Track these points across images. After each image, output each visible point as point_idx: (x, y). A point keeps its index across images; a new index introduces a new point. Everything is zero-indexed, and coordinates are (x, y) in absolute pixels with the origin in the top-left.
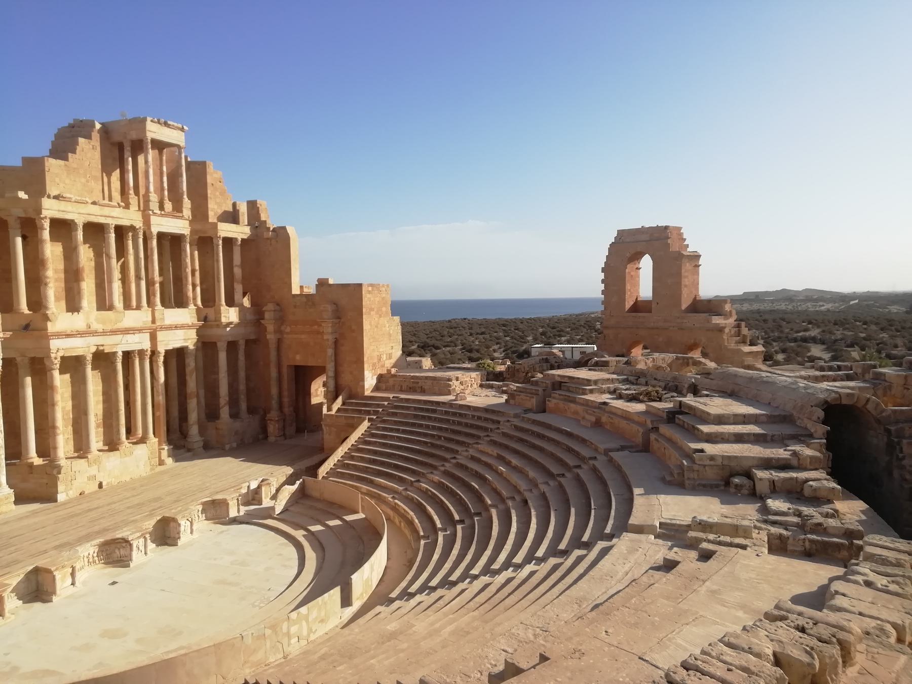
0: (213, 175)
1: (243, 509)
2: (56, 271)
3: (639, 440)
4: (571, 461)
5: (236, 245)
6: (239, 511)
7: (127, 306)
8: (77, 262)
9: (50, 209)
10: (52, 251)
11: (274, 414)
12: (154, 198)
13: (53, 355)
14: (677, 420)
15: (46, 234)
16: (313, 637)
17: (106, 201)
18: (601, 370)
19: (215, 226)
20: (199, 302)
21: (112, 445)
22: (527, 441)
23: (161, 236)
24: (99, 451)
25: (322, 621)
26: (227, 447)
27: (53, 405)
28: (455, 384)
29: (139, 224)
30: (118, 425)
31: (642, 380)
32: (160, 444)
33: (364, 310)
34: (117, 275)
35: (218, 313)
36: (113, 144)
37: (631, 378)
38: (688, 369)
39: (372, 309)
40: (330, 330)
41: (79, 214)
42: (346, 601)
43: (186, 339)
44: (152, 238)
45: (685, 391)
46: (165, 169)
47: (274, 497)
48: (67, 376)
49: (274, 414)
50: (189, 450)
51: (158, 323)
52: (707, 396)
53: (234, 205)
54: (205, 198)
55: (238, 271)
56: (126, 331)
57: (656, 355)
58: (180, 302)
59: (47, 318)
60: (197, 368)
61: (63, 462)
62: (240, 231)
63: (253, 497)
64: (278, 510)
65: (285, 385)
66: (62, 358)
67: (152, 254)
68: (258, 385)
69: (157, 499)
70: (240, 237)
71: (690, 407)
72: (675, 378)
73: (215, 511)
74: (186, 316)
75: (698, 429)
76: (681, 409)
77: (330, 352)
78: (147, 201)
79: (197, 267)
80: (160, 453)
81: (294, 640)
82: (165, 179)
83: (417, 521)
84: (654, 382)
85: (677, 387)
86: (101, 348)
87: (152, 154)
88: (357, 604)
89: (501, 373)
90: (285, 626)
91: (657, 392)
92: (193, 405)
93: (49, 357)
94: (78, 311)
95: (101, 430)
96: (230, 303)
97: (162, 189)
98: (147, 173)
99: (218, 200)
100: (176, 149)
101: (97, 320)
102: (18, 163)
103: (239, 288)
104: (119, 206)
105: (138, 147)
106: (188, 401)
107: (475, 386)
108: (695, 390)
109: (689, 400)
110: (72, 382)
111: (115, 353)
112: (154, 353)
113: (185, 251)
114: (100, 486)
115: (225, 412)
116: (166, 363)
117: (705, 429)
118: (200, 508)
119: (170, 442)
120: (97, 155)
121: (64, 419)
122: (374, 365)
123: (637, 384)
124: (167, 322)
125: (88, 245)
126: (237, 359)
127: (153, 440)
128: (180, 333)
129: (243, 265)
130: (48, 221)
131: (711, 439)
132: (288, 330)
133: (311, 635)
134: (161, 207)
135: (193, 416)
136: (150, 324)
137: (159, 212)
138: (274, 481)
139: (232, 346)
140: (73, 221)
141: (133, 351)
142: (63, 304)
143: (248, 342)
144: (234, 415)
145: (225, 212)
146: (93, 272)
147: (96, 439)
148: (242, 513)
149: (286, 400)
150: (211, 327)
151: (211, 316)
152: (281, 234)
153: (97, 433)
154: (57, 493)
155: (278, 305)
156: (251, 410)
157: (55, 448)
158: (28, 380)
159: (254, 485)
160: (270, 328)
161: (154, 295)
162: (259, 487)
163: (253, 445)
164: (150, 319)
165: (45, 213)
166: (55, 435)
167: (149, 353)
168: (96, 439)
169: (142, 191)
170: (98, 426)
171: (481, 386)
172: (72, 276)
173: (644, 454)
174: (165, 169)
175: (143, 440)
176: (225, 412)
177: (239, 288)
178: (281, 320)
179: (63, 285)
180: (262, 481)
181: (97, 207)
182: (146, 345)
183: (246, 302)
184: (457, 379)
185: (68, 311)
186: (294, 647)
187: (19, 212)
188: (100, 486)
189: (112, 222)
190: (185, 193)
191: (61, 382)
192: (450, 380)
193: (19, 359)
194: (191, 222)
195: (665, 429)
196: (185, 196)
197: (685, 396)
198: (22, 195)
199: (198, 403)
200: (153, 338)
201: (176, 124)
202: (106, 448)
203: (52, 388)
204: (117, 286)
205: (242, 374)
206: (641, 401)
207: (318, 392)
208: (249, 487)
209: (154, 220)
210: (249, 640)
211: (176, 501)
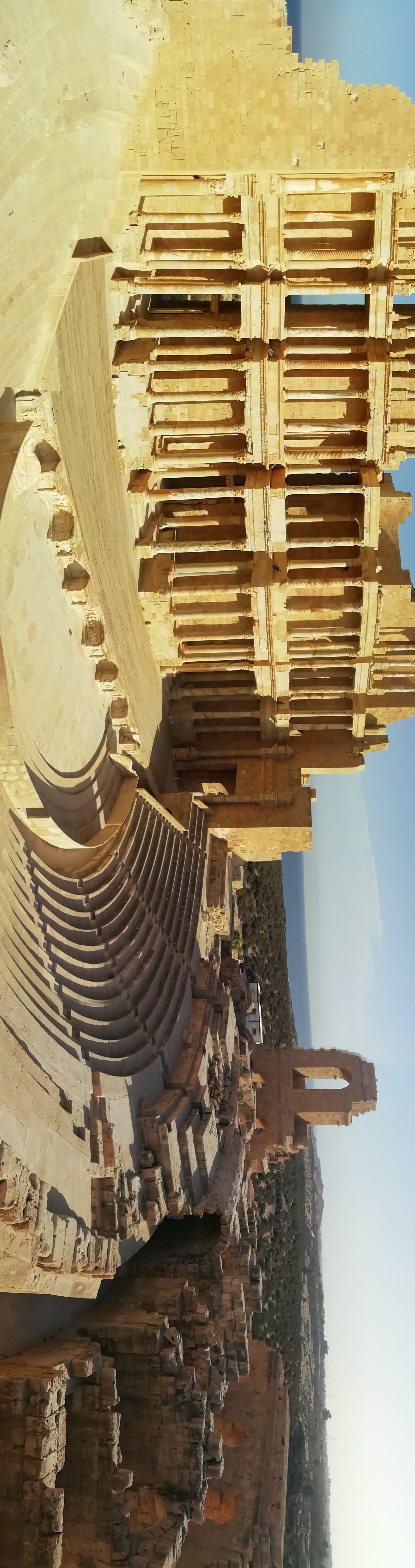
3: (175, 1080)
4: (150, 1021)
14: (194, 1110)
18: (236, 1048)
22: (166, 978)
28: (217, 911)
31: (228, 1083)
37: (230, 1073)
38: (244, 1118)
39: (287, 835)
45: (222, 1116)
52: (219, 1133)
57: (254, 1094)
71: (207, 1121)
72: (233, 1109)
75: (188, 1127)
76: (204, 1115)
84: (227, 1092)
85: (225, 1110)
89: (230, 954)
91: (219, 1095)
107: (217, 930)
108: (223, 1124)
109: (213, 1120)
117: (189, 1132)
123: (225, 1078)
131: (181, 1137)
171: (217, 936)
173: (162, 1084)
184: (222, 913)
192: (221, 906)
195: (185, 1101)
197: (217, 1116)
206: (209, 1082)
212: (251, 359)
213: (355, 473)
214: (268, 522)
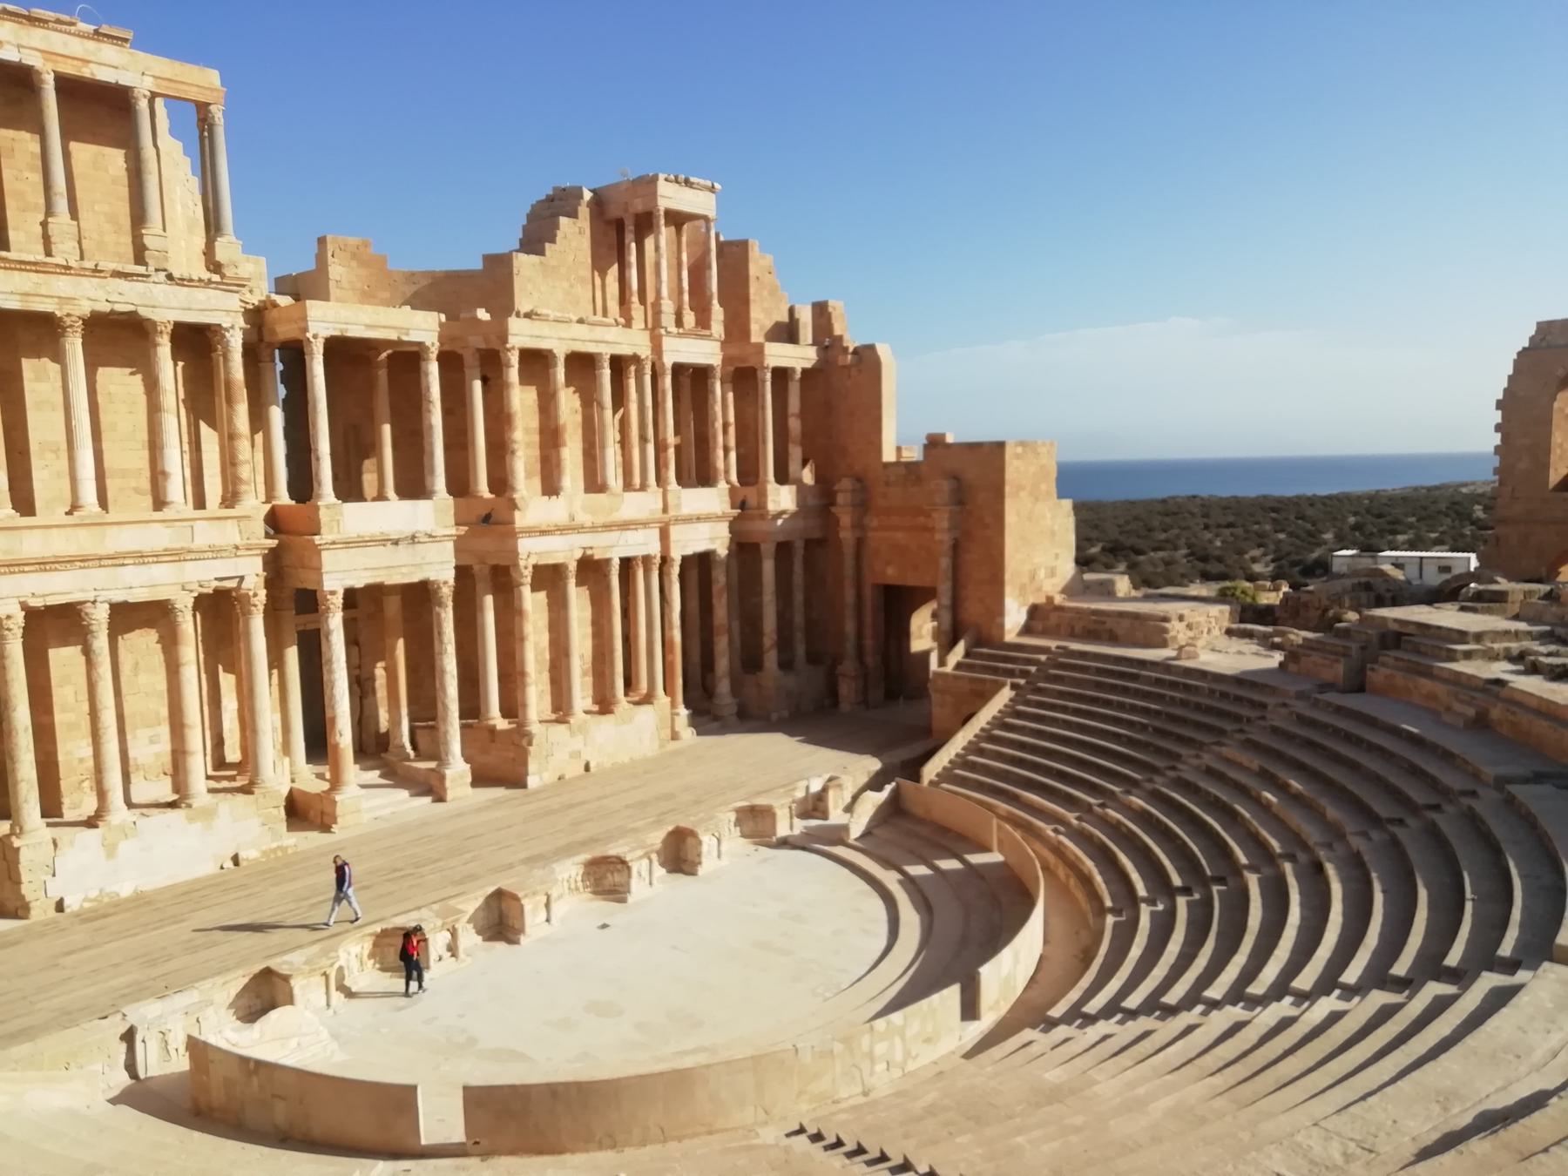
0: (759, 263)
1: (800, 826)
2: (527, 431)
6: (791, 828)
7: (628, 486)
8: (556, 417)
9: (521, 334)
10: (522, 399)
11: (848, 666)
12: (668, 306)
13: (522, 563)
15: (513, 374)
16: (911, 1066)
17: (599, 318)
19: (760, 349)
20: (734, 477)
21: (604, 705)
23: (678, 369)
24: (586, 712)
25: (928, 1040)
26: (774, 716)
27: (522, 639)
28: (1177, 630)
29: (645, 352)
32: (673, 705)
33: (1007, 489)
34: (612, 435)
35: (763, 495)
36: (608, 222)
39: (1022, 488)
40: (945, 524)
41: (560, 341)
42: (970, 1010)
43: (714, 539)
44: (664, 374)
46: (685, 257)
47: (849, 809)
48: (542, 595)
49: (848, 666)
50: (716, 718)
51: (672, 513)
53: (791, 311)
54: (746, 301)
55: (794, 425)
56: (625, 526)
58: (704, 477)
59: (513, 505)
60: (728, 586)
61: (534, 727)
62: (799, 356)
63: (814, 806)
64: (856, 831)
65: (868, 619)
66: (535, 567)
67: (664, 401)
68: (827, 618)
69: (669, 797)
73: (756, 822)
74: (714, 500)
77: (945, 562)
78: (657, 312)
79: (732, 419)
81: (880, 1067)
83: (1098, 879)
86: (589, 552)
87: (665, 233)
88: (989, 1017)
89: (1269, 609)
90: (865, 1041)
92: (722, 644)
93: (516, 565)
94: (557, 494)
95: (589, 679)
96: (782, 477)
97: (681, 292)
98: (657, 265)
100: (702, 223)
102: (478, 265)
103: (796, 453)
104: (617, 324)
105: (645, 224)
106: (716, 639)
107: (1216, 632)
110: (549, 605)
111: (608, 561)
112: (665, 560)
113: (714, 392)
114: (587, 768)
115: (771, 659)
116: (682, 576)
118: (733, 816)
119: (687, 705)
120: (585, 243)
121: (537, 661)
122: (1023, 588)
124: (686, 511)
125: (572, 389)
126: (790, 572)
127: (662, 699)
128: (704, 529)
129: (803, 415)
132: (875, 523)
133: (910, 1062)
134: (679, 322)
135: (722, 664)
136: (659, 515)
137: (673, 329)
138: (847, 780)
140: (550, 351)
141: (634, 558)
142: (537, 483)
143: (809, 544)
144: (786, 665)
145: (778, 325)
146: (580, 431)
147: (582, 694)
148: (797, 832)
149: (869, 643)
151: (752, 501)
152: (867, 358)
153: (582, 684)
154: (526, 774)
155: (859, 480)
156: (813, 658)
157: (524, 706)
158: (489, 600)
159: (816, 786)
160: (845, 519)
161: (666, 466)
162: (825, 790)
163: (816, 718)
164: (660, 506)
166: (524, 686)
167: (658, 561)
168: (582, 694)
169: (651, 297)
170: (584, 674)
172: (550, 437)
174: (685, 257)
175: (648, 699)
176: (771, 659)
177: (796, 453)
178: (863, 505)
179: (537, 452)
180: (830, 780)
181: (584, 326)
182: (655, 549)
183: (808, 476)
184: (1181, 618)
185: (544, 493)
186: (882, 1081)
187: (476, 341)
188: (587, 768)
189: (606, 351)
191: (533, 604)
192: (1166, 619)
193: (476, 568)
196: (715, 301)
198: (483, 315)
199: (731, 642)
200: (664, 536)
201: (702, 181)
202: (596, 708)
203: (520, 612)
204: (612, 454)
205: (799, 598)
207: (922, 631)
208: (808, 788)
209: (668, 343)
210: (806, 1058)
211: (697, 802)
213: (276, 352)
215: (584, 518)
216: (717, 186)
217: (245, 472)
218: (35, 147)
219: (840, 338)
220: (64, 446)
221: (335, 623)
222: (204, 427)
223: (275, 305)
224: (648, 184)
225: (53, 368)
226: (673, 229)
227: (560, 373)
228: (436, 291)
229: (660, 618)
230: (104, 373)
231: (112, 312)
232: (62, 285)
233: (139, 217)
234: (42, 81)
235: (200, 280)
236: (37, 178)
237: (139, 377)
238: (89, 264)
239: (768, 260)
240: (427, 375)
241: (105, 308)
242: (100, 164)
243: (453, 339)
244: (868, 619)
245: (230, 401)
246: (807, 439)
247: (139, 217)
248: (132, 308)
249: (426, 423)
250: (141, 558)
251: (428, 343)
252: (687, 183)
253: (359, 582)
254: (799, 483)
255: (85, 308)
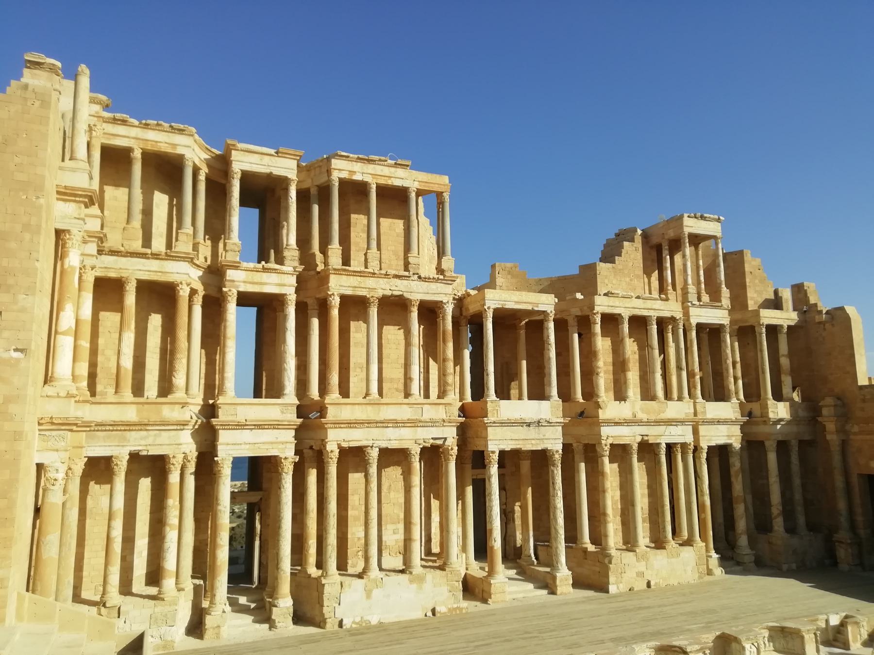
0: (751, 263)
5: (781, 332)
8: (624, 353)
9: (602, 305)
10: (602, 344)
15: (598, 328)
19: (756, 313)
20: (742, 397)
30: (664, 521)
41: (625, 308)
46: (701, 263)
49: (843, 535)
53: (776, 292)
54: (744, 287)
55: (785, 362)
56: (669, 422)
62: (786, 317)
70: (786, 324)
80: (707, 561)
82: (702, 273)
86: (646, 438)
87: (688, 250)
94: (625, 400)
97: (699, 283)
99: (757, 289)
100: (712, 241)
101: (642, 410)
103: (787, 381)
105: (675, 246)
111: (658, 444)
120: (639, 255)
127: (699, 544)
129: (791, 355)
130: (600, 316)
139: (782, 446)
140: (620, 315)
142: (611, 394)
145: (767, 300)
149: (860, 519)
150: (757, 424)
152: (839, 319)
155: (839, 399)
165: (597, 309)
172: (620, 366)
174: (701, 263)
175: (689, 543)
177: (787, 381)
179: (611, 377)
183: (796, 397)
185: (615, 400)
187: (576, 311)
190: (724, 283)
194: (731, 312)
198: (579, 296)
201: (712, 216)
212: (323, 442)
214: (525, 422)
215: (642, 416)
216: (721, 218)
217: (450, 379)
218: (366, 222)
219: (816, 305)
220: (365, 366)
221: (494, 470)
222: (431, 362)
223: (469, 295)
224: (678, 220)
225: (364, 326)
226: (693, 248)
227: (626, 327)
228: (553, 286)
229: (695, 488)
230: (386, 328)
231: (392, 295)
232: (371, 282)
233: (407, 248)
234: (371, 188)
235: (434, 278)
236: (365, 236)
237: (402, 331)
238: (383, 272)
239: (757, 262)
240: (547, 329)
241: (389, 293)
242: (393, 227)
243: (562, 311)
244: (857, 500)
245: (444, 341)
246: (794, 372)
247: (407, 248)
248: (401, 293)
249: (546, 356)
250: (396, 424)
251: (549, 311)
252: (702, 218)
253: (508, 447)
254: (791, 400)
255: (380, 293)
